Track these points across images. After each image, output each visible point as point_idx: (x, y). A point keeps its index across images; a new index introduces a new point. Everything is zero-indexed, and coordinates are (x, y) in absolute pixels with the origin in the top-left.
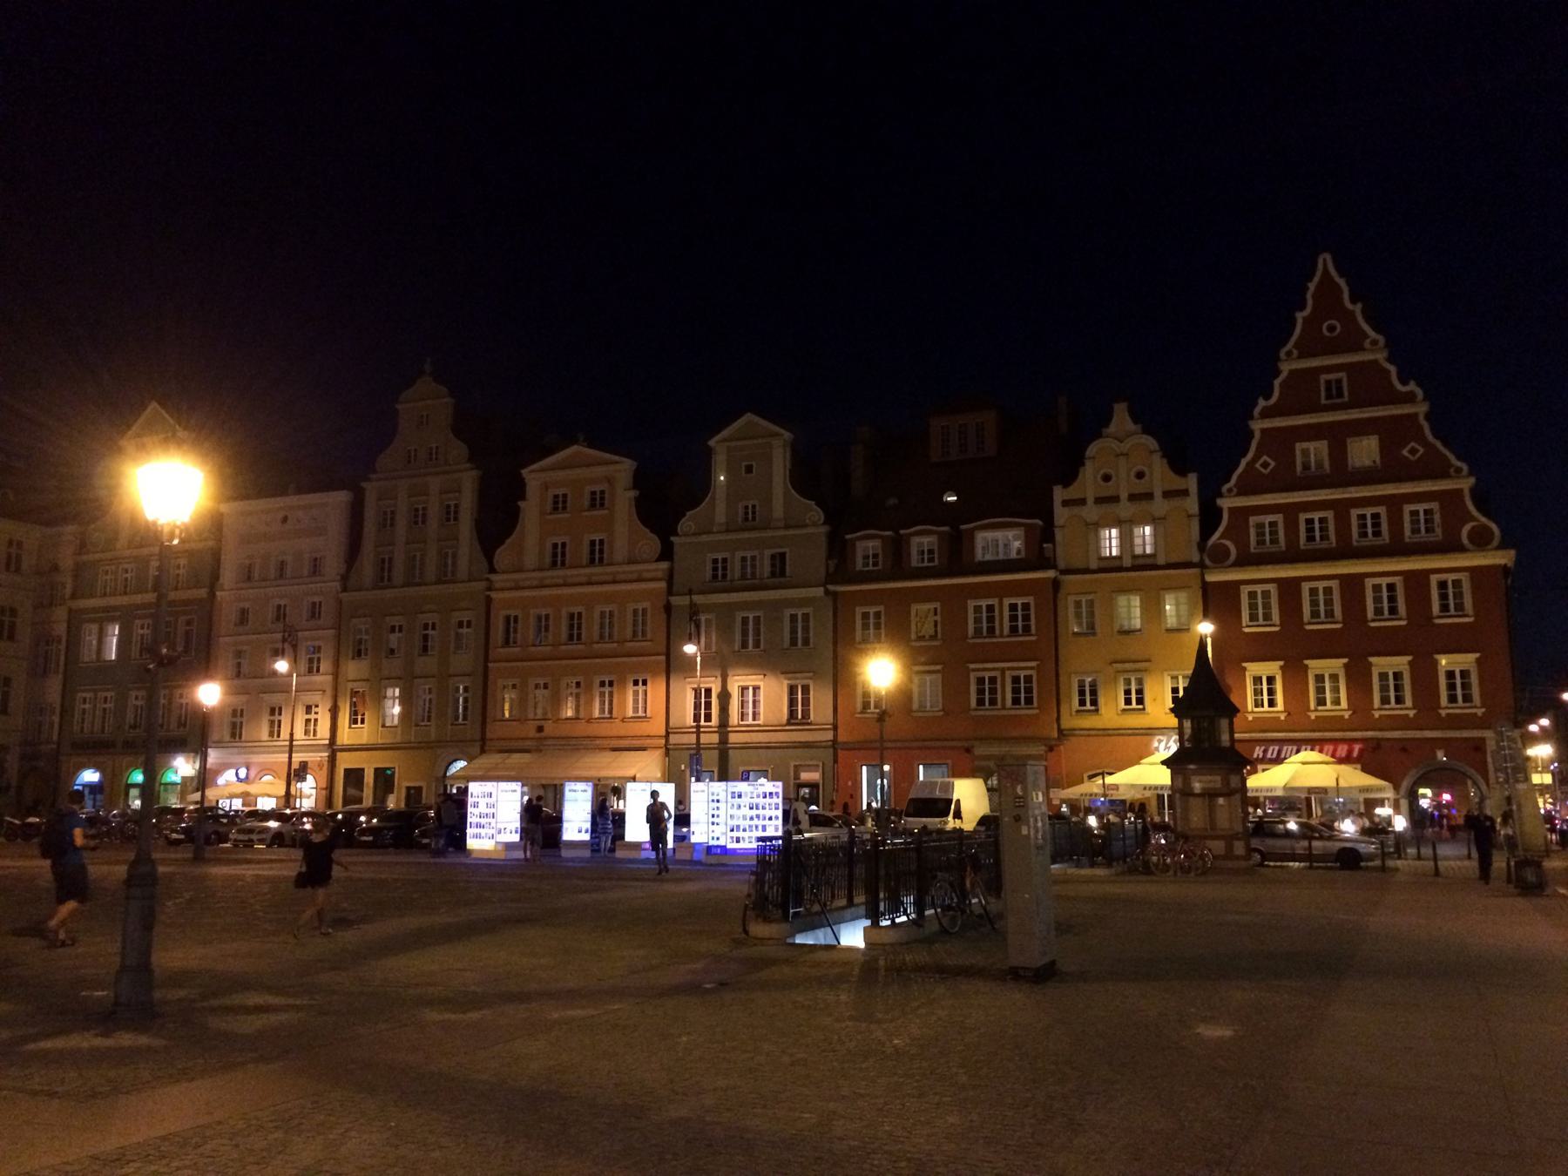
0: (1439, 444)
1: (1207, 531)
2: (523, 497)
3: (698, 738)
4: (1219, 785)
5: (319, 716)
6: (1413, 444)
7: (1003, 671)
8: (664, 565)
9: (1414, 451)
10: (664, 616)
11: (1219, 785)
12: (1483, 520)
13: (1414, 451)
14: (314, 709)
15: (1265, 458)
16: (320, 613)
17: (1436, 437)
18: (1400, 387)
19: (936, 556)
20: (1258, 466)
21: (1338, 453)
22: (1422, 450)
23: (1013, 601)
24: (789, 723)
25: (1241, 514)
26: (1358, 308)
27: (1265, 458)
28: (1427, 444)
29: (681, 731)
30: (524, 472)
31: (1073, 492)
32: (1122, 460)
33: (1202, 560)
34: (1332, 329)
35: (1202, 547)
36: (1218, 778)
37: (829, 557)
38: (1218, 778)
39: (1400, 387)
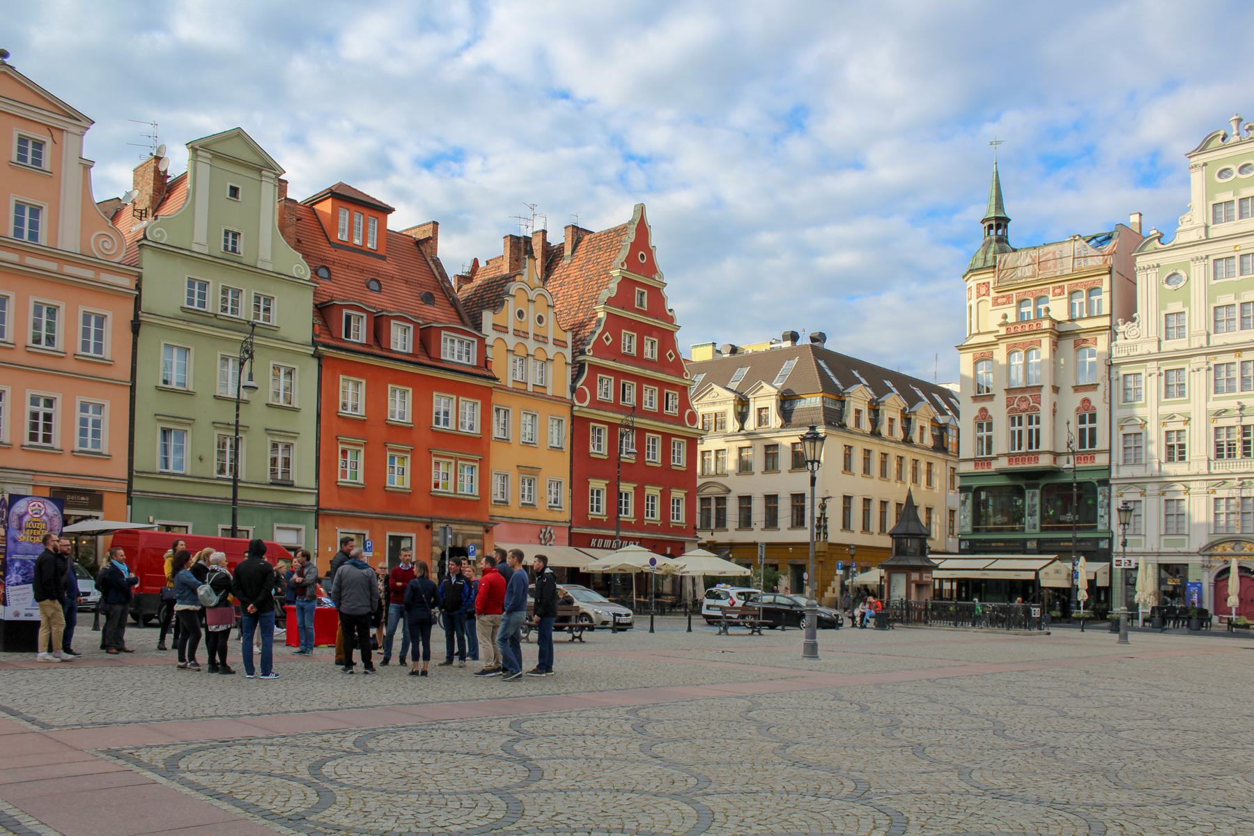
1: (575, 379)
9: (671, 356)
10: (130, 336)
13: (671, 356)
15: (607, 334)
20: (604, 338)
24: (272, 484)
25: (595, 369)
27: (607, 334)
31: (500, 318)
32: (531, 306)
33: (572, 400)
35: (573, 390)
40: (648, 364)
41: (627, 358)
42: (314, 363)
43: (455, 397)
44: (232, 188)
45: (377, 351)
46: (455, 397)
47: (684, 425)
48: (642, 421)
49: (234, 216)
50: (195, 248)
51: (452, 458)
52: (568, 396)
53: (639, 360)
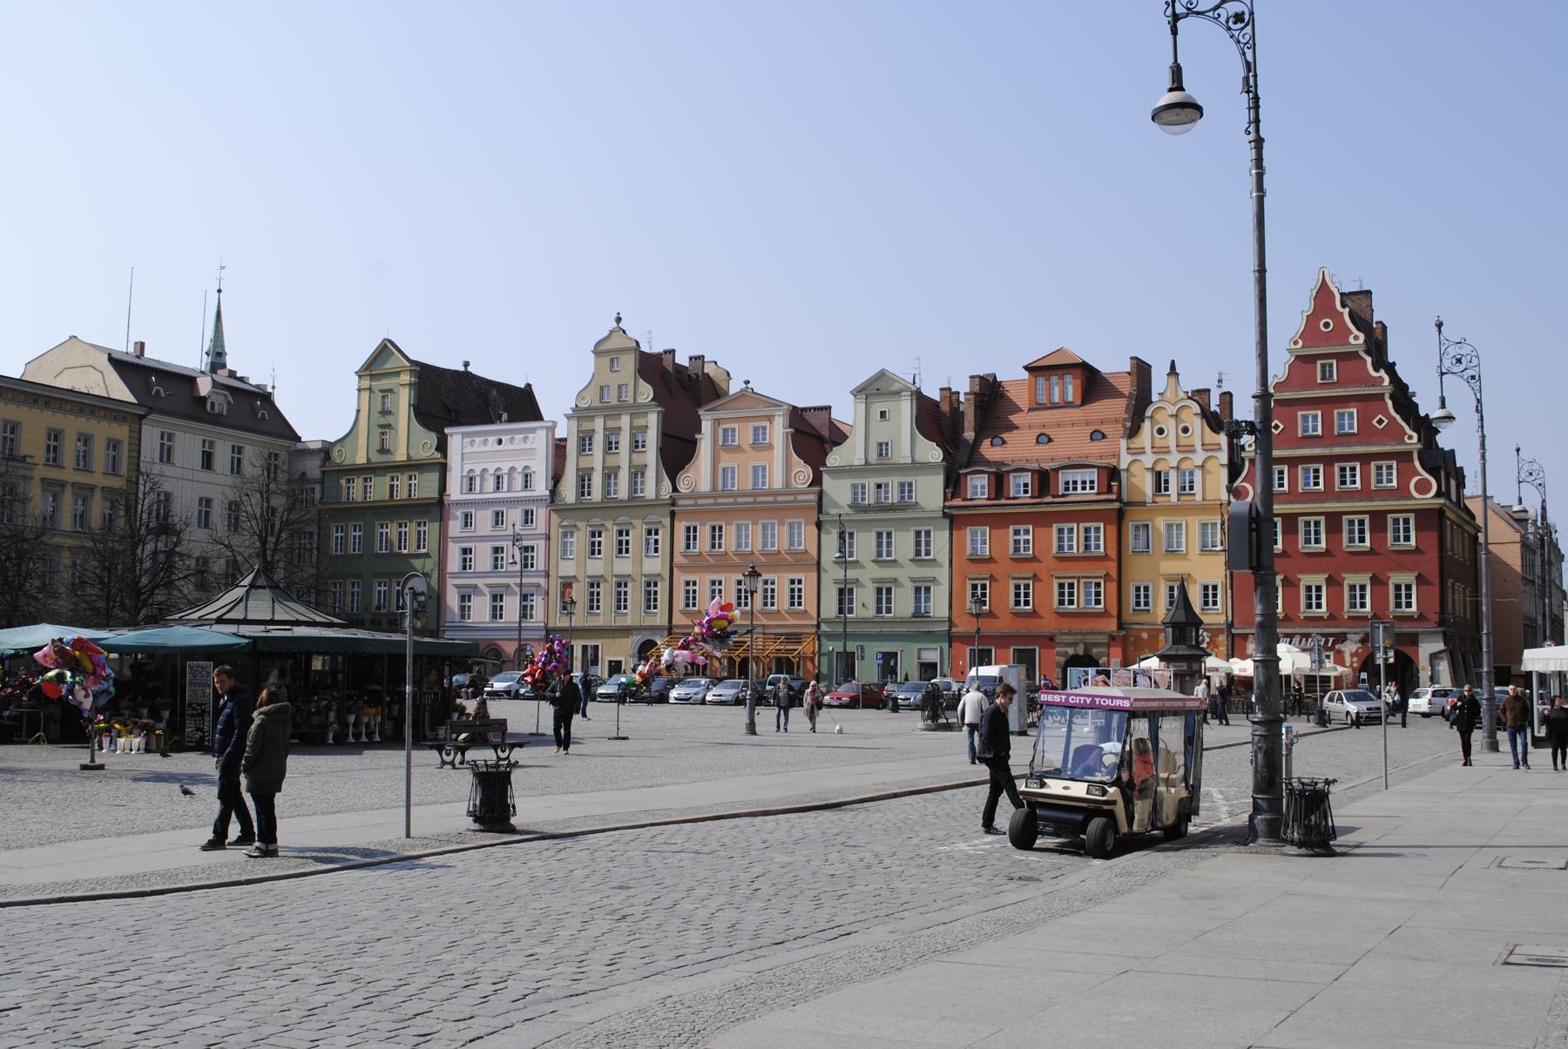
0: (1398, 418)
1: (1233, 476)
2: (699, 431)
3: (845, 628)
4: (1185, 668)
5: (534, 603)
6: (1380, 416)
7: (1078, 579)
8: (817, 489)
11: (1185, 668)
12: (1426, 475)
13: (1380, 421)
14: (529, 598)
16: (532, 519)
17: (1397, 412)
18: (1374, 374)
19: (1030, 489)
21: (1328, 423)
22: (1386, 421)
23: (1088, 525)
26: (1346, 311)
28: (1391, 419)
29: (827, 622)
30: (701, 412)
34: (1327, 325)
35: (1230, 490)
36: (1185, 664)
37: (946, 487)
38: (1185, 664)
39: (1374, 374)
40: (1346, 438)
41: (1310, 440)
42: (946, 522)
43: (1075, 525)
44: (881, 412)
45: (1003, 501)
46: (1075, 525)
47: (1411, 497)
48: (1326, 505)
49: (881, 432)
50: (856, 463)
51: (1074, 578)
52: (1224, 496)
53: (1328, 437)
